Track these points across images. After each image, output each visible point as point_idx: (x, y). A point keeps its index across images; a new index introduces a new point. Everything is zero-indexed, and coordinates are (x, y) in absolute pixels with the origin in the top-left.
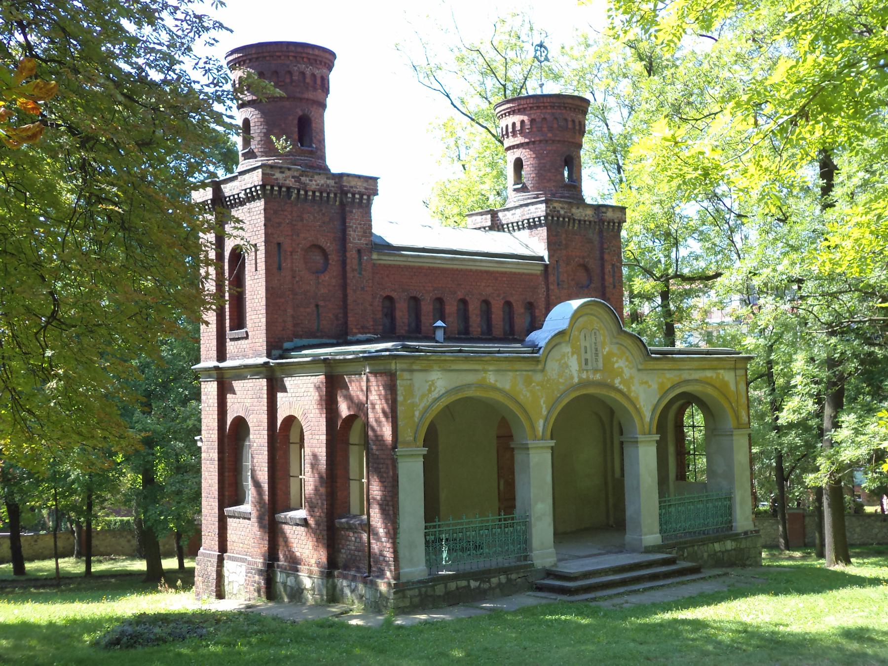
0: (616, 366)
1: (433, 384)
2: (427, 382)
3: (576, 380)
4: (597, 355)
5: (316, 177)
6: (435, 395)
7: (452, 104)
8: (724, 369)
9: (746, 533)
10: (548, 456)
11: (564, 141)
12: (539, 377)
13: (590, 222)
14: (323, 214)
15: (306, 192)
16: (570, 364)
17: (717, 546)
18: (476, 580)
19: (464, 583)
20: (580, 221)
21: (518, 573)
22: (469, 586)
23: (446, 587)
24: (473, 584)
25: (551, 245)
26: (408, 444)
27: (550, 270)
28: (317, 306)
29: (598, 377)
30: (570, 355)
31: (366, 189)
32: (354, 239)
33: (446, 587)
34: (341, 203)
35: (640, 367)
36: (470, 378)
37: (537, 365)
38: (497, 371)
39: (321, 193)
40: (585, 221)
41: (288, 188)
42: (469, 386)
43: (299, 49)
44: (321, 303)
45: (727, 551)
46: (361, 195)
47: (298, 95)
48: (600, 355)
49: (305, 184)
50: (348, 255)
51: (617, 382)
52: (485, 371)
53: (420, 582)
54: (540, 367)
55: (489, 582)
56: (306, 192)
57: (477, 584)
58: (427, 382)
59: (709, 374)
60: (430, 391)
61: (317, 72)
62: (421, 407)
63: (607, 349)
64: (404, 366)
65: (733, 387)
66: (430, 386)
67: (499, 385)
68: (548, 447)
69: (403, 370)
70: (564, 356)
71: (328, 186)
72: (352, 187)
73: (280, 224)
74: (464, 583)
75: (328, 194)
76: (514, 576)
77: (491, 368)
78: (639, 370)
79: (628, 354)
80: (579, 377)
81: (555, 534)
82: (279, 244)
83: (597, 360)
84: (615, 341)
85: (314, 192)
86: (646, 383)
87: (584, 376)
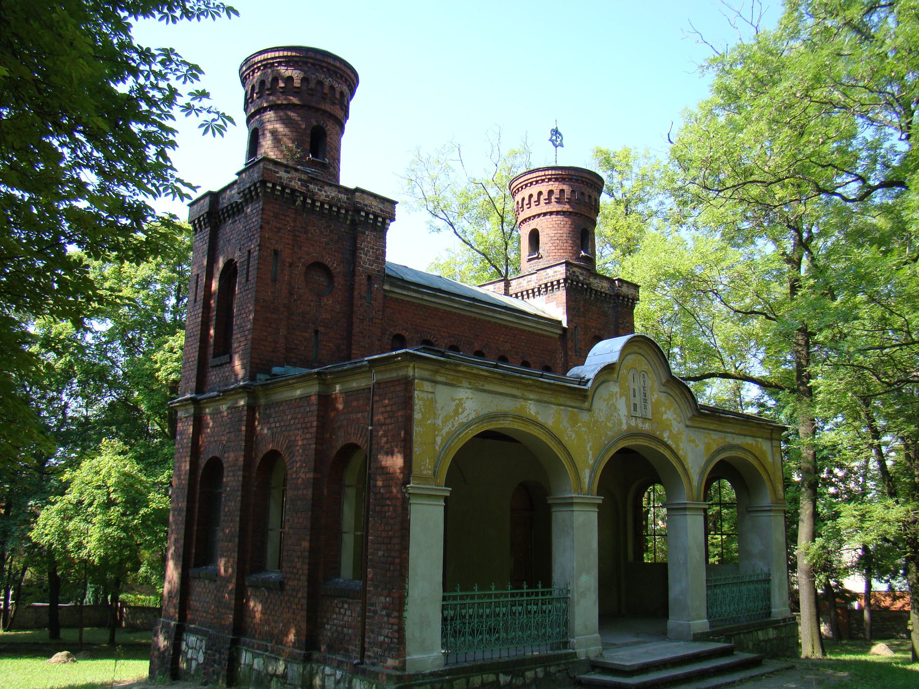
0: (665, 417)
1: (460, 404)
2: (453, 400)
3: (624, 427)
4: (645, 401)
5: (326, 188)
6: (462, 419)
7: (455, 232)
8: (762, 438)
9: (784, 620)
10: (593, 516)
11: (581, 215)
12: (585, 416)
13: (606, 294)
14: (331, 231)
15: (314, 201)
16: (618, 406)
17: (761, 635)
18: (506, 674)
19: (491, 678)
20: (596, 291)
21: (558, 665)
22: (498, 681)
23: (468, 682)
24: (503, 679)
25: (570, 310)
26: (425, 479)
27: (569, 335)
28: (316, 332)
29: (646, 427)
30: (618, 396)
31: (382, 210)
32: (365, 263)
33: (468, 682)
34: (353, 221)
35: (688, 423)
36: (507, 405)
37: (584, 402)
38: (538, 401)
39: (331, 207)
40: (601, 293)
41: (293, 191)
42: (505, 415)
43: (319, 57)
44: (321, 329)
45: (770, 640)
46: (376, 216)
47: (314, 104)
48: (649, 402)
49: (314, 194)
50: (357, 279)
51: (665, 436)
52: (526, 399)
53: (432, 674)
54: (586, 405)
55: (523, 676)
56: (314, 201)
57: (508, 678)
58: (453, 400)
59: (749, 440)
60: (456, 413)
62: (444, 432)
63: (655, 396)
64: (426, 374)
65: (770, 459)
66: (457, 406)
67: (540, 419)
68: (594, 504)
69: (423, 379)
70: (611, 396)
71: (339, 200)
72: (366, 205)
73: (279, 229)
74: (491, 678)
75: (339, 209)
76: (553, 669)
77: (532, 396)
78: (687, 426)
79: (676, 405)
80: (627, 423)
81: (601, 616)
82: (276, 253)
83: (646, 408)
84: (663, 389)
85: (322, 204)
86: (693, 441)
87: (633, 423)
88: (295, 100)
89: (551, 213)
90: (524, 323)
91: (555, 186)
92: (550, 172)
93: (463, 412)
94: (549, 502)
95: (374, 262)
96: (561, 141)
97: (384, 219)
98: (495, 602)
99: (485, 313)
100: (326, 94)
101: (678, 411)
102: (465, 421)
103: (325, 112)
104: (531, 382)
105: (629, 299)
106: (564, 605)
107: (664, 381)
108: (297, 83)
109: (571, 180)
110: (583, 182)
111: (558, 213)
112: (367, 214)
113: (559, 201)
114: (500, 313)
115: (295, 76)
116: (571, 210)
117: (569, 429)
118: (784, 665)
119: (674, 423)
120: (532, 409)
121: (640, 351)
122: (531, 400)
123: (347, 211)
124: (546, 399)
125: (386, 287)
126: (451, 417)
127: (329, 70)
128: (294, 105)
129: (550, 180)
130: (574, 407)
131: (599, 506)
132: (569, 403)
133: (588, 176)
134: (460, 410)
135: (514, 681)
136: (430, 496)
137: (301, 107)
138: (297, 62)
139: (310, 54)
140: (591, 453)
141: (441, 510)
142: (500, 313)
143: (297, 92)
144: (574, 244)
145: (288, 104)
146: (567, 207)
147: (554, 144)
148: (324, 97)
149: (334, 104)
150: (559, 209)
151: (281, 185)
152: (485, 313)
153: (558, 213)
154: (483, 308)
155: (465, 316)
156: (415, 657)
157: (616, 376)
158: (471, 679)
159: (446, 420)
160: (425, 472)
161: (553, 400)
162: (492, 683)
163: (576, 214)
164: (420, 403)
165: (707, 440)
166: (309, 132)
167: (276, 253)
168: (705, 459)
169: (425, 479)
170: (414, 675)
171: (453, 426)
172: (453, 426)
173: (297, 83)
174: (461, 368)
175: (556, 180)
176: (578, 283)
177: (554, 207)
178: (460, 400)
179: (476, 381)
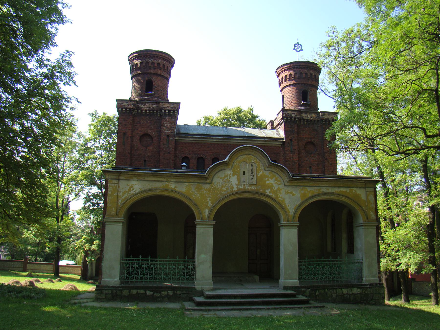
0: (267, 182)
1: (132, 186)
2: (128, 185)
3: (235, 189)
4: (252, 176)
5: (147, 104)
6: (133, 192)
8: (357, 187)
9: (371, 285)
10: (211, 230)
11: (302, 84)
12: (207, 186)
13: (315, 120)
14: (151, 120)
15: (142, 111)
16: (231, 180)
17: (345, 291)
18: (150, 291)
19: (142, 291)
20: (307, 120)
21: (182, 291)
22: (146, 293)
23: (130, 292)
24: (148, 293)
25: (286, 132)
26: (112, 216)
27: (286, 144)
28: (145, 161)
29: (253, 188)
30: (232, 175)
31: (172, 108)
32: (165, 130)
33: (130, 292)
34: (160, 114)
35: (286, 184)
36: (158, 185)
37: (207, 180)
38: (176, 182)
39: (150, 111)
40: (311, 120)
41: (130, 109)
42: (156, 189)
43: (145, 53)
44: (147, 159)
45: (353, 294)
46: (169, 111)
47: (145, 72)
48: (255, 176)
49: (141, 108)
50: (162, 138)
51: (267, 192)
52: (169, 182)
53: (113, 287)
54: (208, 181)
55: (160, 293)
56: (142, 111)
57: (152, 293)
58: (128, 185)
59: (343, 190)
60: (130, 190)
61: (155, 61)
62: (123, 198)
63: (261, 173)
64: (114, 177)
65: (363, 197)
66: (130, 188)
67: (177, 189)
68: (211, 224)
69: (112, 179)
70: (227, 176)
71: (153, 108)
72: (164, 107)
73: (126, 125)
74: (142, 291)
75: (153, 111)
76: (178, 292)
77: (172, 180)
78: (285, 186)
79: (277, 176)
80: (237, 187)
81: (213, 273)
82: (124, 134)
83: (252, 179)
84: (267, 169)
85: (146, 111)
86: (291, 193)
87: (242, 187)
88: (139, 72)
89: (287, 86)
90: (257, 142)
91: (287, 73)
92: (284, 67)
93: (133, 190)
94: (196, 223)
95: (170, 129)
96: (301, 48)
97: (174, 111)
98: (178, 264)
99: (232, 141)
100: (150, 66)
101: (279, 178)
102: (134, 193)
103: (151, 73)
104: (169, 175)
105: (329, 121)
106: (192, 267)
107: (267, 165)
108: (139, 65)
109: (294, 68)
110: (301, 68)
111: (290, 85)
112: (165, 111)
113: (290, 80)
114: (241, 140)
115: (138, 63)
116: (295, 83)
117: (196, 192)
118: (319, 305)
119: (274, 185)
120: (173, 186)
121: (251, 153)
122: (172, 182)
123: (157, 111)
124: (182, 181)
125: (177, 138)
126: (127, 192)
127: (150, 56)
128: (139, 74)
129: (285, 70)
130: (200, 183)
131: (298, 226)
132: (196, 181)
133: (303, 64)
134: (132, 189)
135: (155, 294)
136: (115, 222)
137: (141, 74)
138: (138, 57)
139: (142, 53)
140: (210, 202)
141: (212, 229)
142: (241, 140)
143: (139, 69)
144: (298, 99)
145: (137, 74)
146: (293, 82)
147: (297, 51)
148: (150, 68)
149: (155, 69)
150: (290, 84)
151: (125, 108)
152: (232, 141)
153: (290, 85)
154: (230, 139)
155: (222, 144)
156: (106, 280)
157: (230, 166)
158: (131, 291)
159: (125, 193)
160: (112, 213)
161: (186, 181)
162: (143, 294)
163: (299, 84)
164: (111, 188)
165: (303, 192)
166: (145, 83)
167: (124, 134)
168: (300, 201)
169: (112, 216)
170: (104, 286)
171: (128, 195)
172: (128, 195)
173: (139, 65)
174: (129, 173)
175: (287, 70)
176: (291, 118)
177: (288, 83)
178: (132, 185)
179: (139, 177)
